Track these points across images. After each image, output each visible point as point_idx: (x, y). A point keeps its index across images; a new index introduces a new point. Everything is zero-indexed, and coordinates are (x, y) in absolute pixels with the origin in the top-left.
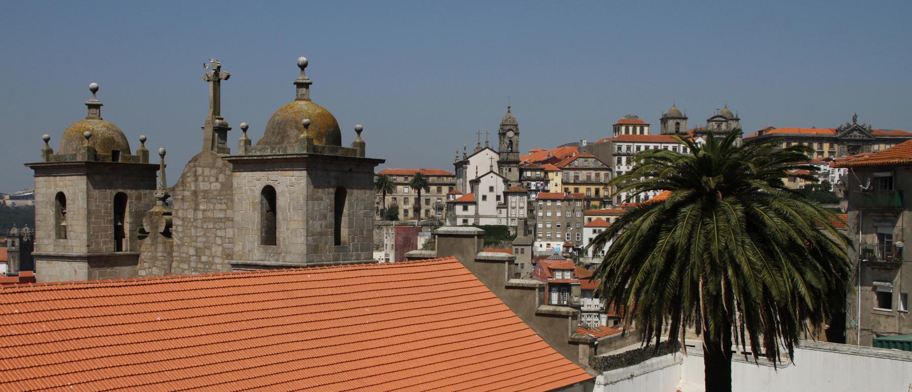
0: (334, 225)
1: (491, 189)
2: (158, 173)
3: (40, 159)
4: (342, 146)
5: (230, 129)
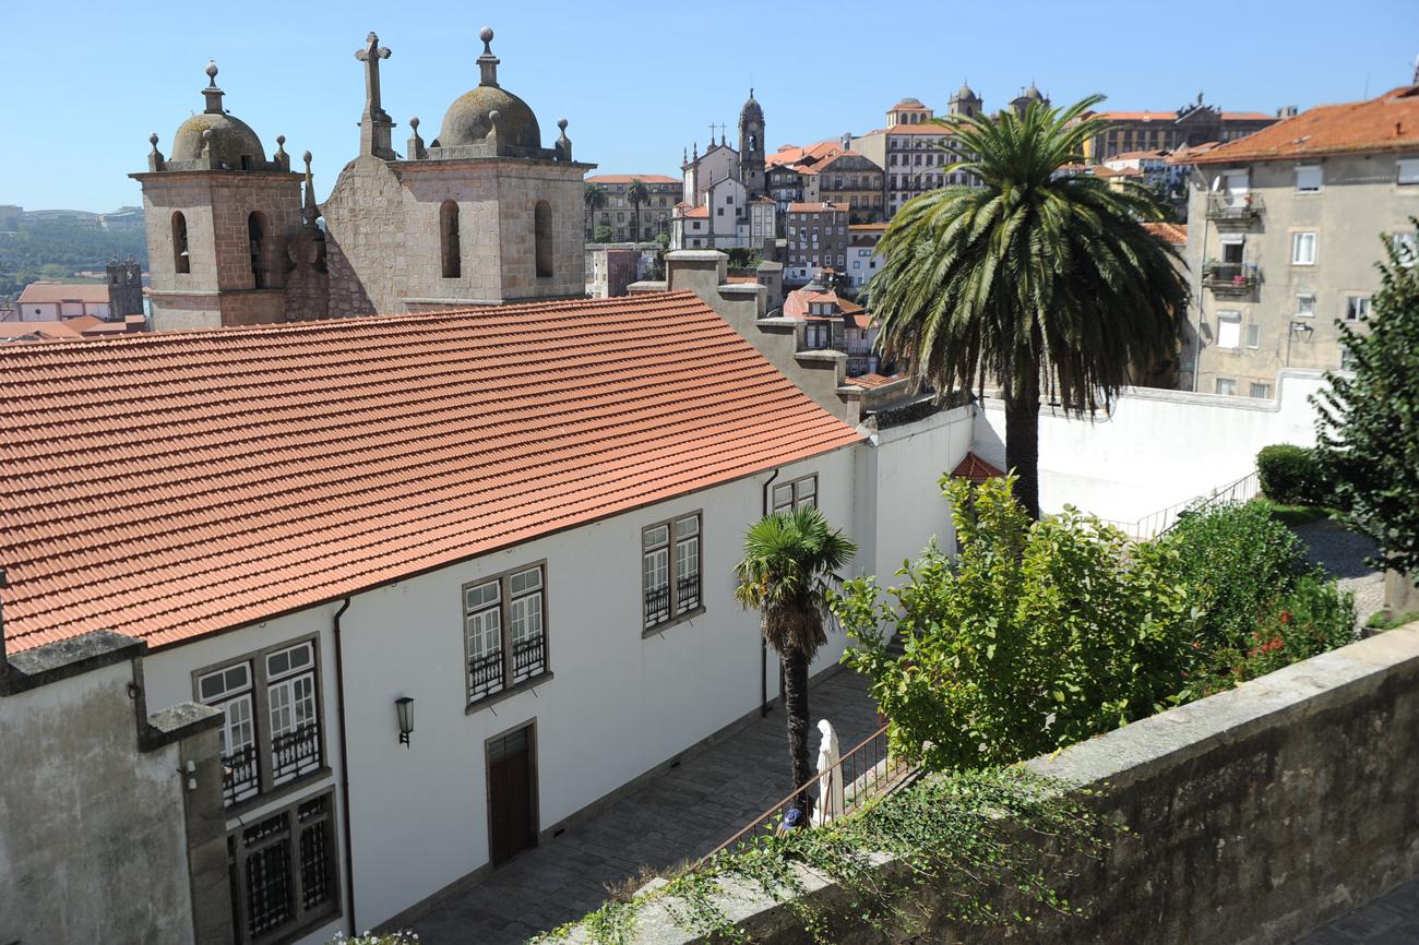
1: (730, 200)
2: (303, 184)
3: (145, 167)
4: (543, 147)
5: (395, 125)
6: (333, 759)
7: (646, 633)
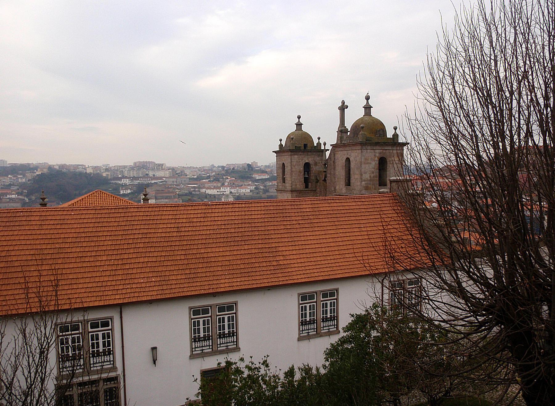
0: (378, 176)
6: (119, 364)
7: (300, 339)
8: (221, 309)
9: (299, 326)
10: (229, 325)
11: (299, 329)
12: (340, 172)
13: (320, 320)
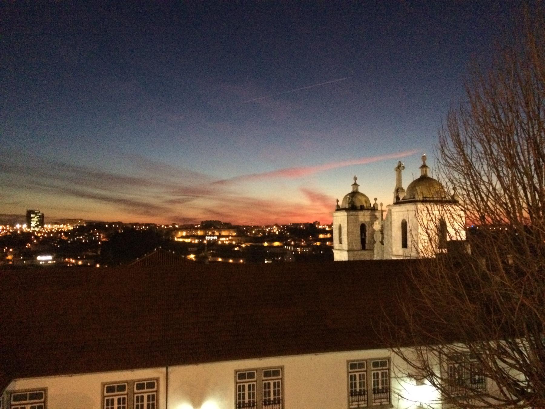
8: (267, 374)
9: (348, 397)
10: (275, 391)
11: (349, 400)
12: (396, 233)
13: (370, 392)
